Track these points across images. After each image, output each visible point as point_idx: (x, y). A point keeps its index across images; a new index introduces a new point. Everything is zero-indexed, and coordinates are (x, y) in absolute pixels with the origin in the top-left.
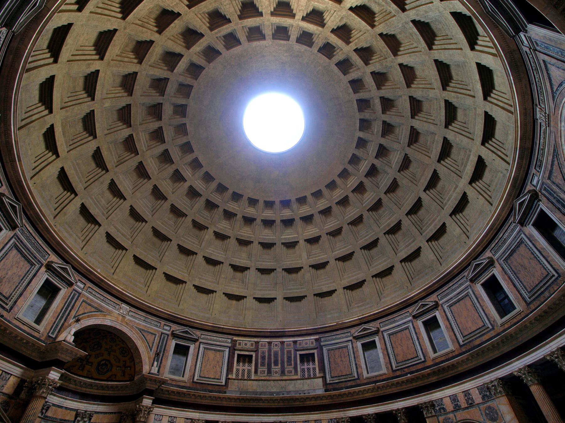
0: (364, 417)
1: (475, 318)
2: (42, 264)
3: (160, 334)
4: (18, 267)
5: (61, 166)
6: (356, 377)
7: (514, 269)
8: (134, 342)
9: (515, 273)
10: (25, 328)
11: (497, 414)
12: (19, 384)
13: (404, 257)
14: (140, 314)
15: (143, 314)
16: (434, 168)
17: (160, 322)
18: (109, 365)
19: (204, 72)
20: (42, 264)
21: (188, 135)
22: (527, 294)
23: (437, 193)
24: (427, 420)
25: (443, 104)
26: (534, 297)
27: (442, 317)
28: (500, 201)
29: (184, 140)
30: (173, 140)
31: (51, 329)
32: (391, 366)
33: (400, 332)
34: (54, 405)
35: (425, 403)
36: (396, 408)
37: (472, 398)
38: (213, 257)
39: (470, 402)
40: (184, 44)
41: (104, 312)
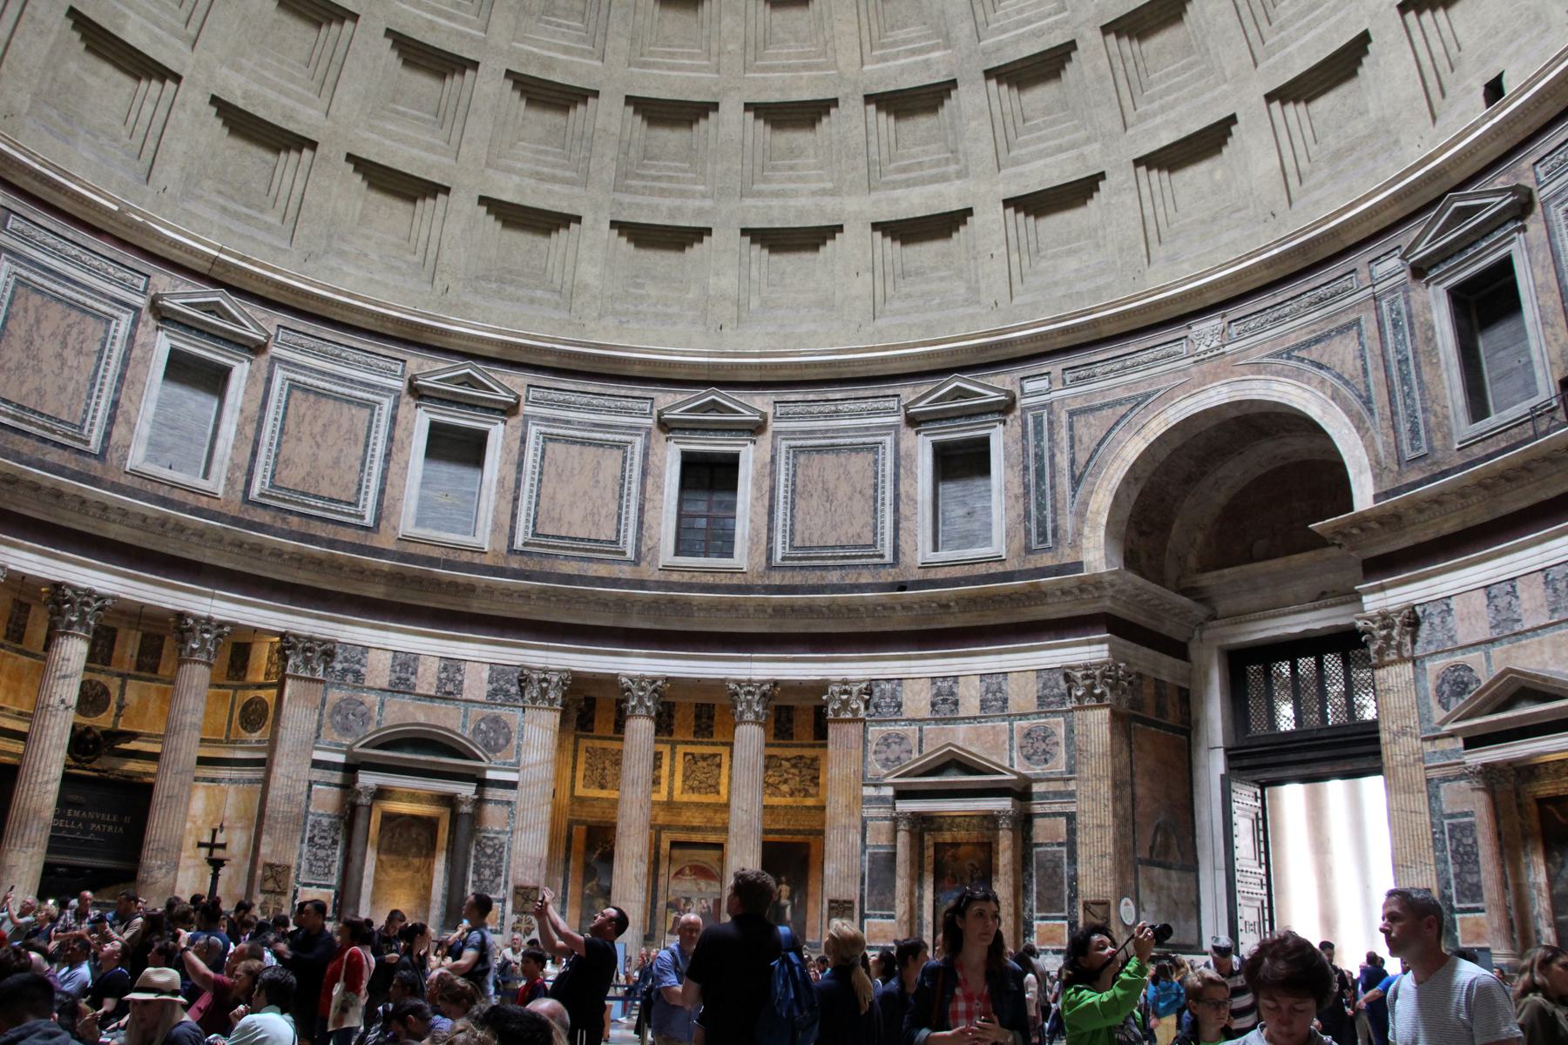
0: (69, 592)
1: (604, 512)
6: (95, 445)
7: (799, 482)
9: (793, 491)
11: (508, 741)
13: (507, 197)
16: (839, 94)
22: (784, 548)
23: (766, 146)
24: (289, 682)
25: (1057, 39)
26: (796, 563)
27: (506, 448)
28: (924, 344)
32: (248, 484)
33: (336, 399)
35: (310, 639)
36: (205, 614)
37: (461, 682)
39: (450, 687)
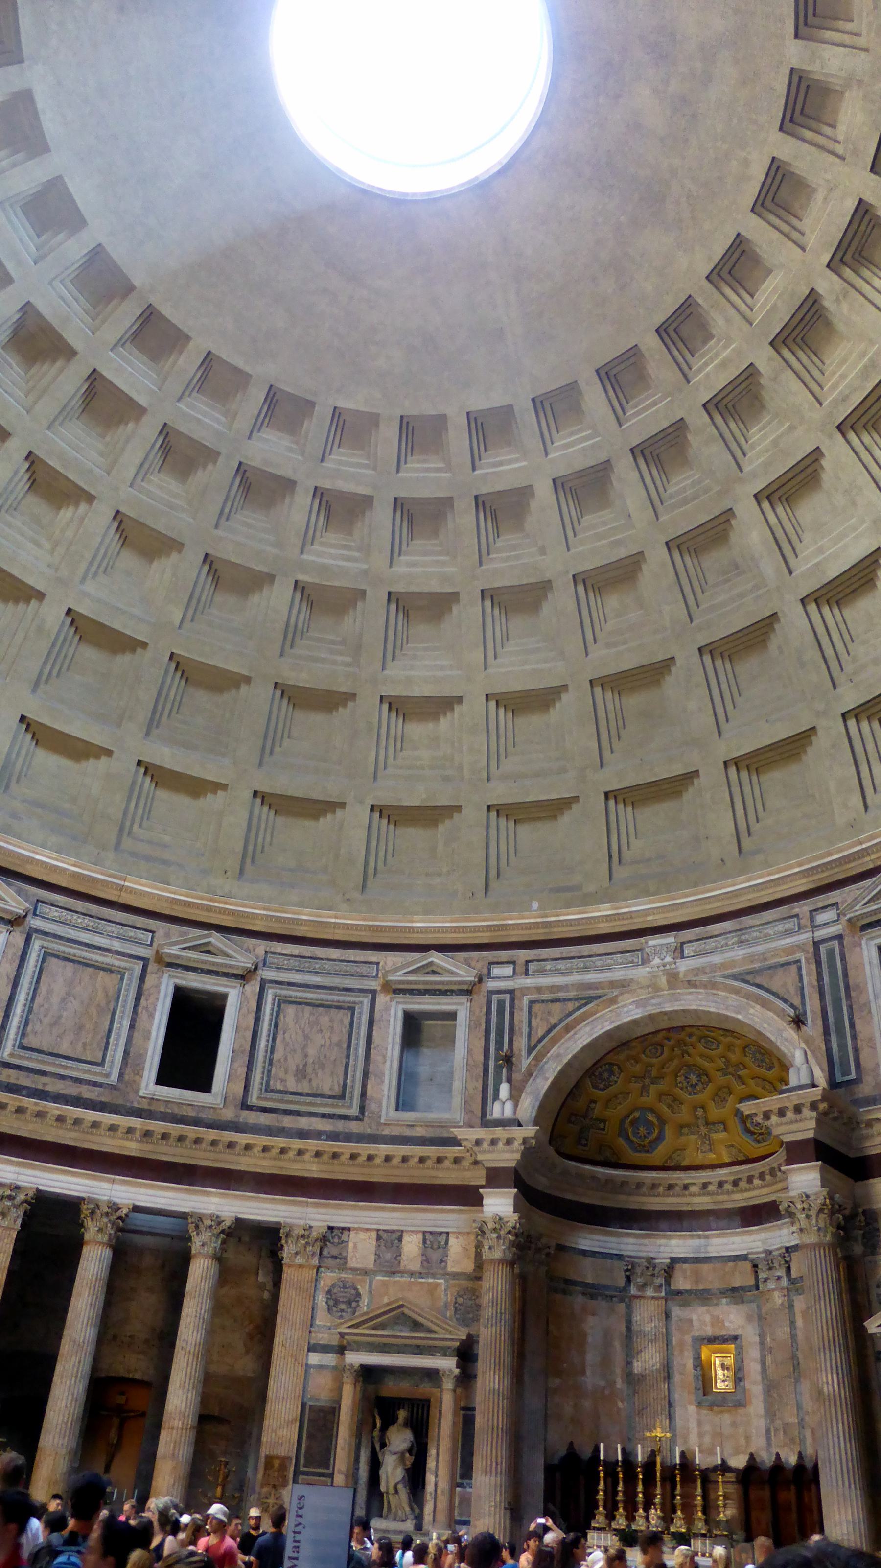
2: (373, 993)
3: (812, 950)
4: (321, 1031)
5: (248, 794)
8: (738, 1020)
10: (419, 1132)
15: (727, 925)
17: (796, 911)
19: (166, 310)
20: (373, 993)
21: (378, 415)
29: (389, 432)
30: (375, 469)
34: (684, 1260)
38: (834, 571)
40: (59, 364)
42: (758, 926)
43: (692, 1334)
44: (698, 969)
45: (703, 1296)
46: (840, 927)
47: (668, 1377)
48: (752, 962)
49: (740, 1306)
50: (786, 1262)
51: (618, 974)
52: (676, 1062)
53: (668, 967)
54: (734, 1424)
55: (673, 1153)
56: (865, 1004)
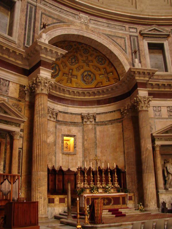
3: (129, 37)
8: (106, 47)
12: (20, 89)
14: (101, 21)
17: (124, 25)
18: (92, 76)
31: (24, 40)
41: (66, 23)
42: (113, 24)
43: (62, 133)
44: (95, 28)
45: (65, 123)
46: (137, 34)
47: (55, 145)
48: (111, 33)
49: (76, 127)
50: (95, 117)
51: (71, 19)
52: (72, 54)
53: (86, 24)
54: (72, 159)
55: (60, 80)
56: (143, 55)
